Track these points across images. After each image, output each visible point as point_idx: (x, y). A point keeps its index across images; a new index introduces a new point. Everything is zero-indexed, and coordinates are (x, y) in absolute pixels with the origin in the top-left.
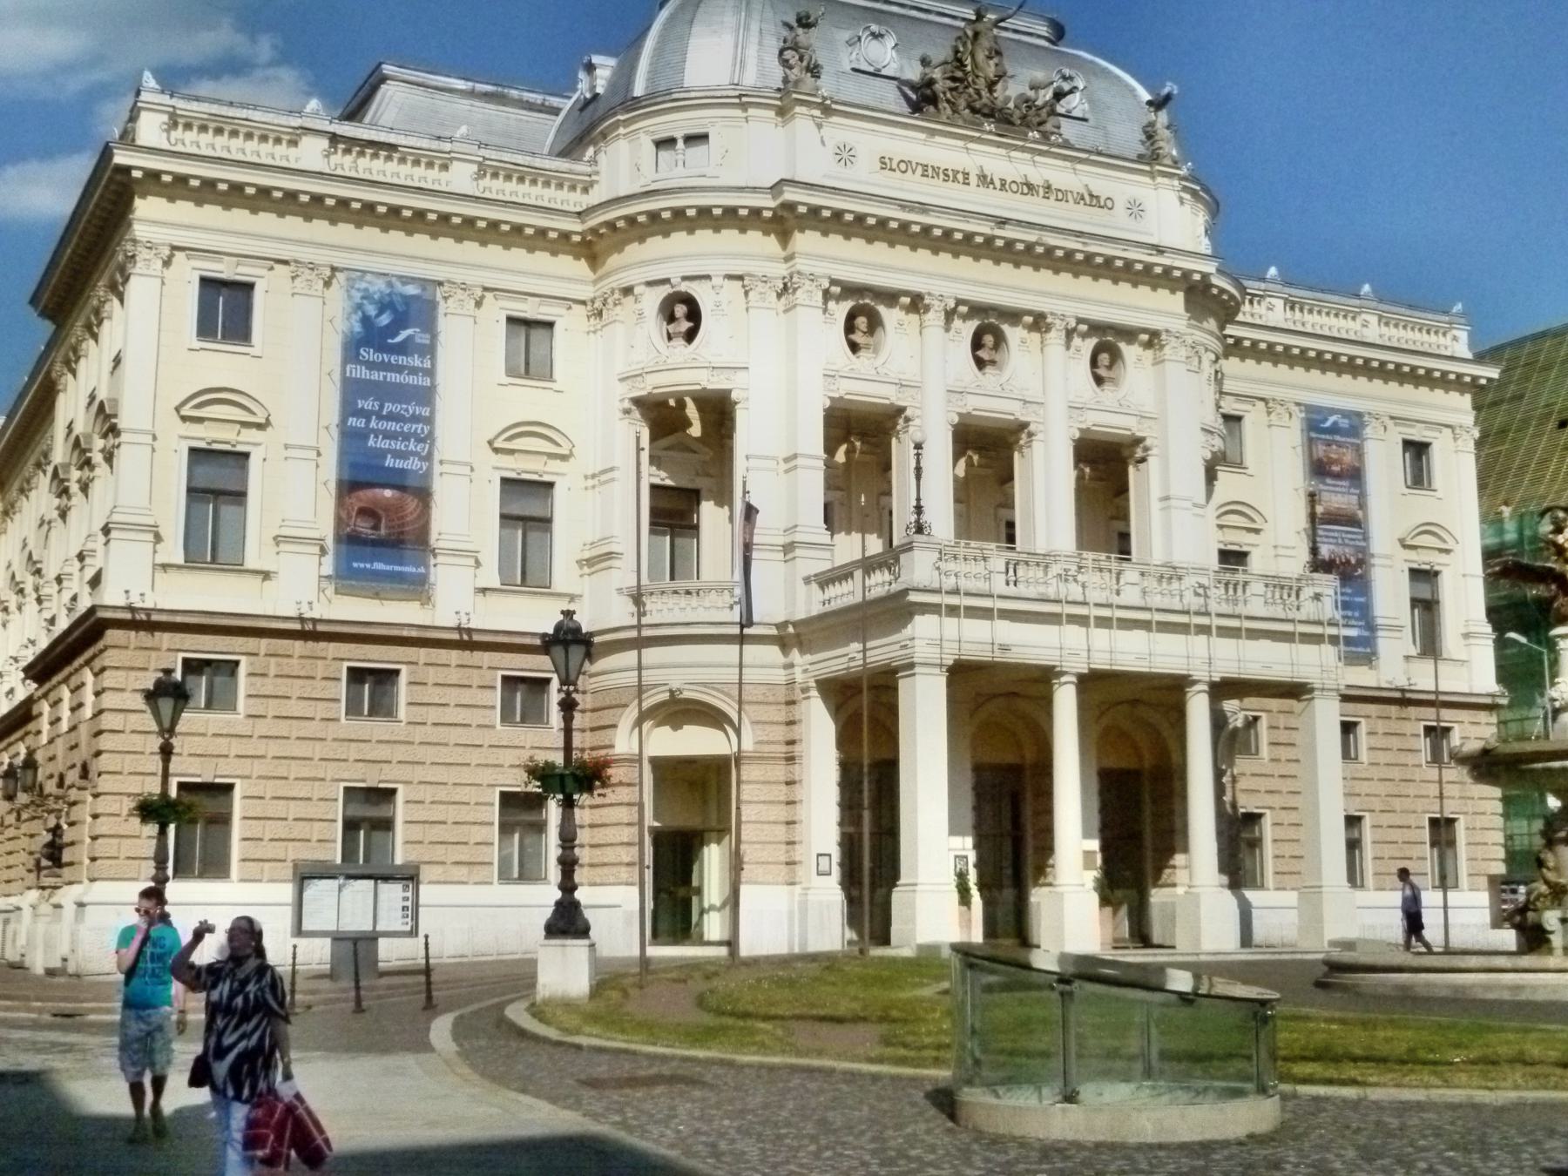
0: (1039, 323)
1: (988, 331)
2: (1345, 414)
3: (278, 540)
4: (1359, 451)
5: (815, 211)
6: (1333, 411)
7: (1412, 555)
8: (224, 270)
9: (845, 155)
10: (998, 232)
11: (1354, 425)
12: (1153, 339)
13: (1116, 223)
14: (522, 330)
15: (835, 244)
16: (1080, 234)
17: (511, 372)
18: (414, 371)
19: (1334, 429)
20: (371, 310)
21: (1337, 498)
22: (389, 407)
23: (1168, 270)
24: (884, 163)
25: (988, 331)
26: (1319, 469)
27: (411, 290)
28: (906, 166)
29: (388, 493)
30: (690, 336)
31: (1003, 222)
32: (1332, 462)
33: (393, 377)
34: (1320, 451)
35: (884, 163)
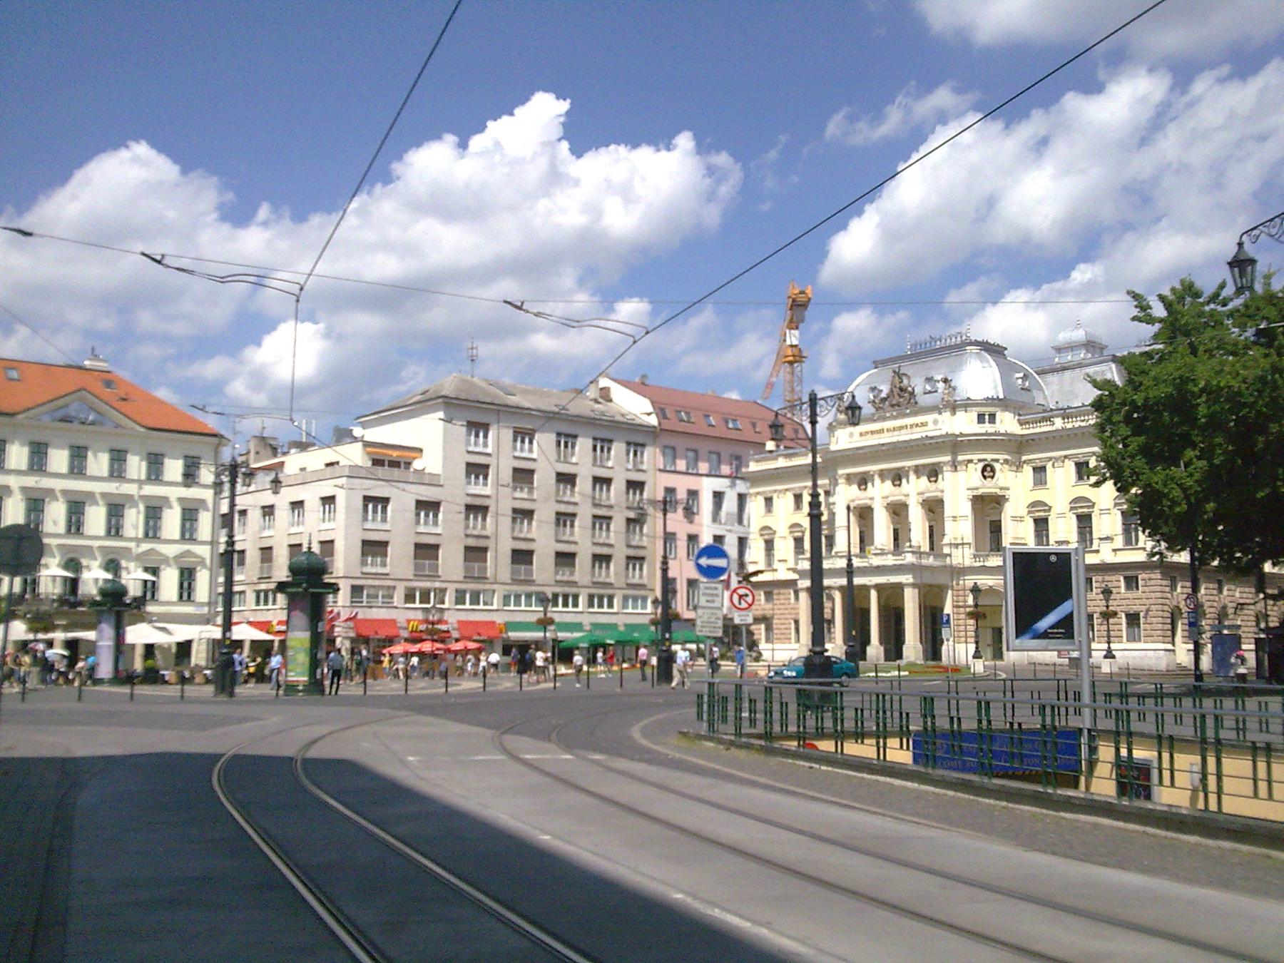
9: (851, 435)
24: (861, 435)
35: (861, 435)
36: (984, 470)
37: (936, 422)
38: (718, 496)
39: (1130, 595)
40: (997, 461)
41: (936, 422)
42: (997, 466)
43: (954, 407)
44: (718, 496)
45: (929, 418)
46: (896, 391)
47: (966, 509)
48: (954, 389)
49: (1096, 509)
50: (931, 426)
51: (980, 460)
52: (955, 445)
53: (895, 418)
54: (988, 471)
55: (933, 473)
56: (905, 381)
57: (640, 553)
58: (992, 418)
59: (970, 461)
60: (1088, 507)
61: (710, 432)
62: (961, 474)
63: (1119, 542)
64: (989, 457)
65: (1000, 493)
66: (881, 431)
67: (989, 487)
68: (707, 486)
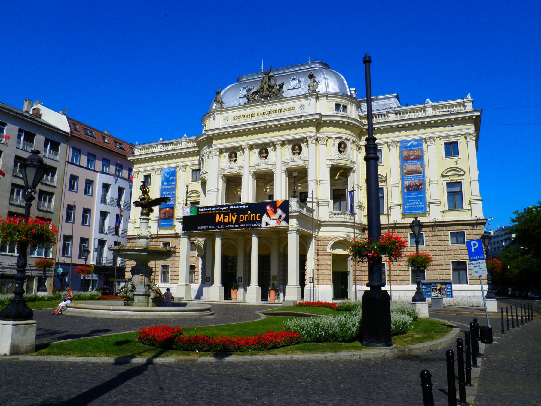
1: (263, 150)
2: (415, 140)
4: (422, 150)
5: (213, 135)
6: (411, 140)
7: (447, 179)
8: (147, 173)
9: (226, 119)
10: (255, 126)
11: (419, 144)
13: (297, 112)
14: (195, 172)
15: (219, 141)
16: (276, 120)
18: (172, 185)
19: (412, 146)
20: (166, 175)
21: (413, 166)
22: (168, 193)
25: (263, 150)
26: (405, 159)
27: (172, 169)
28: (240, 117)
29: (167, 209)
31: (256, 124)
32: (410, 156)
33: (169, 187)
34: (405, 153)
36: (339, 146)
37: (302, 107)
39: (457, 247)
40: (348, 140)
41: (302, 107)
42: (349, 144)
43: (318, 96)
44: (106, 187)
45: (296, 104)
46: (266, 86)
47: (326, 175)
48: (318, 83)
51: (337, 138)
54: (342, 147)
55: (297, 146)
57: (48, 216)
58: (345, 107)
61: (105, 146)
63: (445, 206)
64: (344, 136)
65: (351, 165)
67: (341, 160)
68: (99, 179)
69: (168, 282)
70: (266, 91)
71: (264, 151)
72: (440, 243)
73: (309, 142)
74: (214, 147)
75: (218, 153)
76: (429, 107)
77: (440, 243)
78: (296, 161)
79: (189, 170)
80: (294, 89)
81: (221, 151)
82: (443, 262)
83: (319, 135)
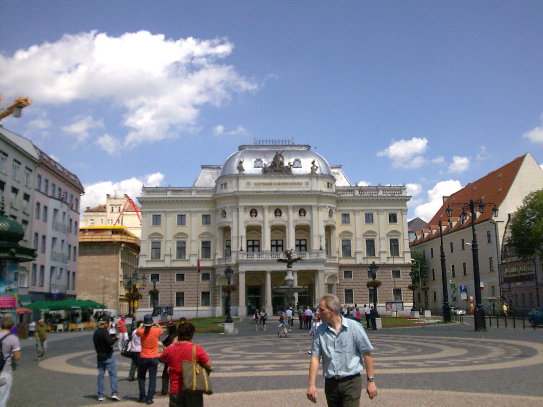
0: (287, 208)
3: (165, 255)
12: (311, 207)
17: (203, 224)
23: (311, 195)
24: (256, 184)
30: (225, 217)
38: (56, 210)
40: (334, 208)
41: (307, 184)
43: (318, 177)
49: (377, 237)
50: (304, 185)
51: (329, 207)
52: (319, 196)
53: (280, 178)
54: (331, 214)
56: (281, 159)
59: (325, 206)
60: (373, 236)
62: (321, 213)
66: (271, 184)
69: (183, 305)
70: (278, 167)
71: (278, 211)
72: (386, 277)
73: (313, 209)
74: (241, 204)
75: (243, 209)
76: (380, 189)
77: (386, 277)
78: (304, 221)
79: (200, 216)
80: (297, 167)
81: (245, 208)
82: (388, 289)
83: (321, 204)
